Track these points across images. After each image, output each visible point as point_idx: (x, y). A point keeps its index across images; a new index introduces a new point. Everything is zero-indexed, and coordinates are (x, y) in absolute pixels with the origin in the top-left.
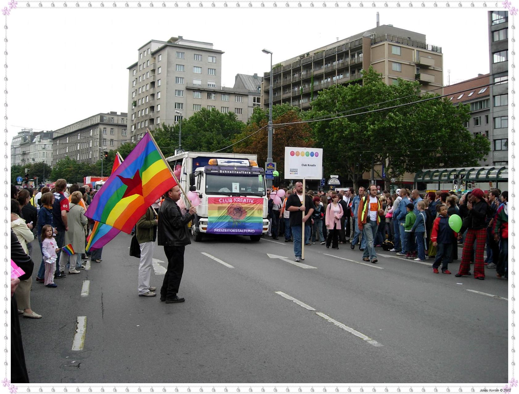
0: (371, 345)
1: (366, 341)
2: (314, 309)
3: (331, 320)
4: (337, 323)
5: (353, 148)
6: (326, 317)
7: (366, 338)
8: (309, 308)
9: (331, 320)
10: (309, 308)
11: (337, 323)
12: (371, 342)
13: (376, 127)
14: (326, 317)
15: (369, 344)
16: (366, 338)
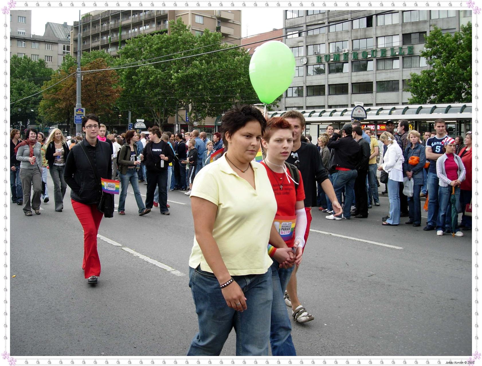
0: (174, 275)
1: (169, 272)
2: (120, 245)
3: (136, 254)
4: (142, 257)
5: (159, 94)
6: (132, 251)
7: (169, 269)
8: (115, 244)
9: (136, 254)
10: (115, 244)
11: (142, 257)
12: (174, 272)
13: (180, 75)
14: (132, 251)
15: (172, 274)
16: (169, 269)
